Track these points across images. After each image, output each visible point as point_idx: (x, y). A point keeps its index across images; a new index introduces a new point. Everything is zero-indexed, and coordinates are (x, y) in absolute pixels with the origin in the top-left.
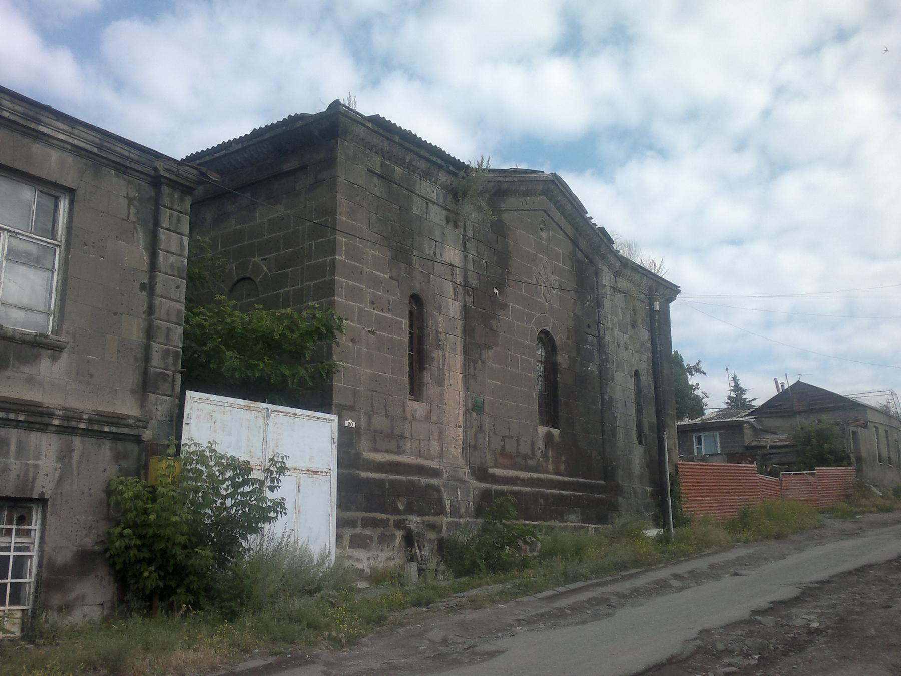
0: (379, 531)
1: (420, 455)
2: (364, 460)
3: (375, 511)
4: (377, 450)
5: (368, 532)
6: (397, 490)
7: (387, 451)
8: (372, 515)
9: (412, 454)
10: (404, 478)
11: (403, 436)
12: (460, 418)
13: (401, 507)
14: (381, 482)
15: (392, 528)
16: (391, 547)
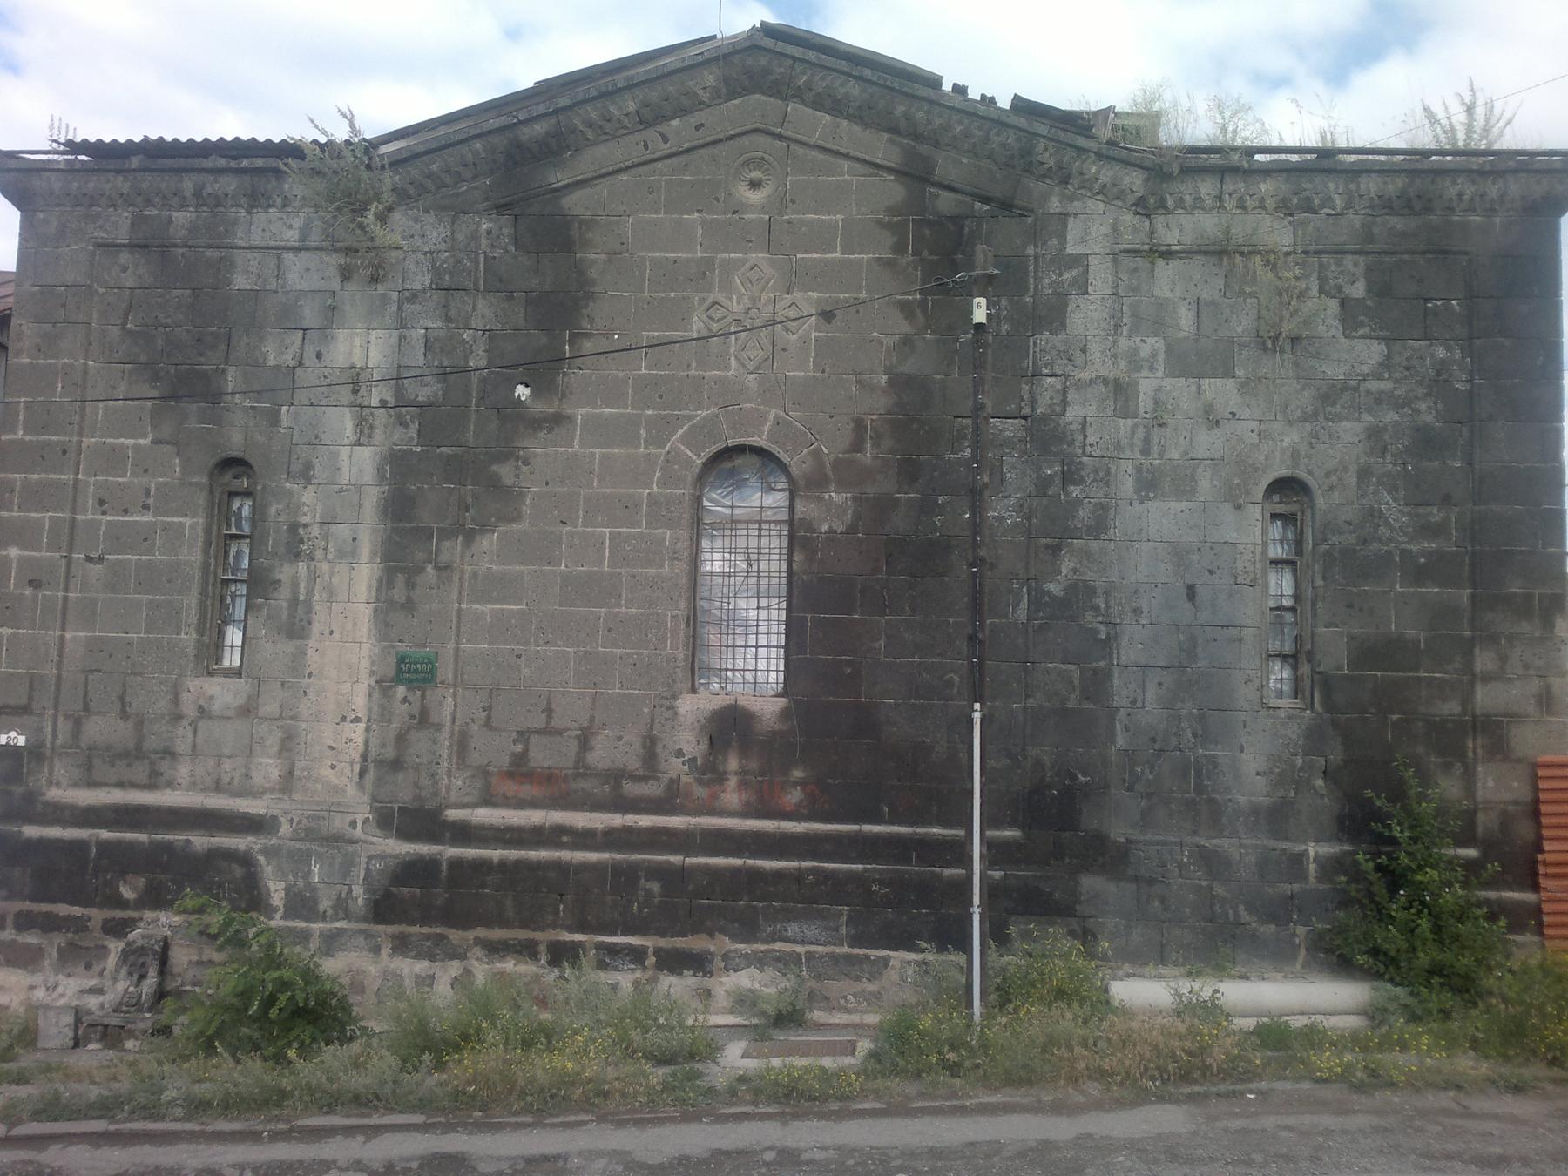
0: (59, 939)
1: (218, 787)
2: (46, 804)
3: (54, 901)
4: (92, 784)
5: (31, 939)
6: (120, 859)
7: (120, 785)
8: (45, 907)
9: (193, 786)
10: (143, 837)
11: (169, 753)
12: (360, 701)
13: (127, 893)
14: (79, 847)
15: (98, 934)
16: (96, 969)
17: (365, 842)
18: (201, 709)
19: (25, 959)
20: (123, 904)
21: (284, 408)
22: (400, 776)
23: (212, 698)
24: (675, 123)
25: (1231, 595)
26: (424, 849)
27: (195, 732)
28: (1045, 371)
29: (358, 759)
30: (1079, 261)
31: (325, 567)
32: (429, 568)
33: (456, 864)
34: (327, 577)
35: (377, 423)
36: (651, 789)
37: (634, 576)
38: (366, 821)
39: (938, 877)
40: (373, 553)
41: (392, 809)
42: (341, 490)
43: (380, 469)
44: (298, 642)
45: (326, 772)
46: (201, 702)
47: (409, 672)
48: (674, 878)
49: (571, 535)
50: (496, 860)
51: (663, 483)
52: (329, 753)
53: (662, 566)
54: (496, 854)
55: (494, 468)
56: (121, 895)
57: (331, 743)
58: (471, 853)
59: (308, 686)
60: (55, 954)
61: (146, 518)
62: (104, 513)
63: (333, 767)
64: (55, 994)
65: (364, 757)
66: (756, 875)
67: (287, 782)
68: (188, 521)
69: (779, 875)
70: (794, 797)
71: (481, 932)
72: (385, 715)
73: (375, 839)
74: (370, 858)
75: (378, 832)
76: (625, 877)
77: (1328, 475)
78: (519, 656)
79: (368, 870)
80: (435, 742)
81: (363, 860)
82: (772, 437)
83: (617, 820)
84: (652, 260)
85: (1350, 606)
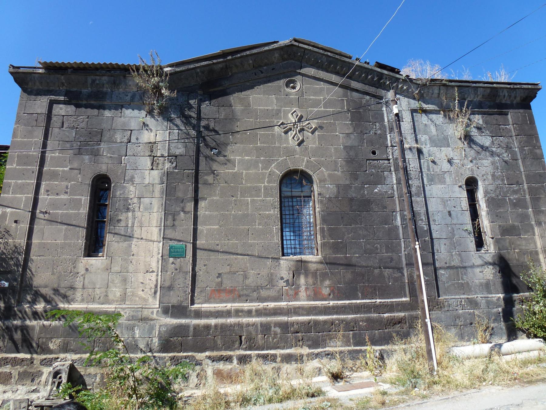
8: (13, 355)
9: (83, 301)
11: (72, 288)
16: (37, 381)
17: (157, 320)
18: (87, 270)
19: (4, 379)
20: (51, 352)
21: (123, 157)
22: (172, 293)
23: (92, 265)
24: (265, 68)
25: (462, 214)
26: (183, 321)
27: (84, 278)
29: (153, 286)
31: (139, 213)
33: (196, 327)
34: (140, 218)
36: (272, 293)
37: (260, 214)
38: (158, 311)
40: (159, 208)
41: (169, 306)
42: (146, 186)
44: (128, 242)
45: (141, 293)
47: (174, 252)
48: (285, 326)
49: (235, 201)
50: (213, 324)
51: (268, 182)
52: (141, 285)
53: (271, 211)
54: (213, 322)
55: (206, 177)
56: (49, 348)
57: (142, 281)
58: (203, 322)
59: (132, 259)
60: (17, 377)
62: (48, 195)
63: (143, 291)
64: (17, 394)
65: (156, 286)
66: (316, 323)
67: (123, 299)
68: (83, 198)
69: (325, 322)
70: (326, 291)
71: (207, 353)
72: (164, 269)
73: (162, 319)
74: (160, 326)
75: (163, 316)
76: (266, 328)
77: (483, 176)
78: (218, 245)
79: (159, 331)
81: (157, 327)
82: (306, 166)
83: (262, 305)
84: (260, 109)
85: (497, 216)
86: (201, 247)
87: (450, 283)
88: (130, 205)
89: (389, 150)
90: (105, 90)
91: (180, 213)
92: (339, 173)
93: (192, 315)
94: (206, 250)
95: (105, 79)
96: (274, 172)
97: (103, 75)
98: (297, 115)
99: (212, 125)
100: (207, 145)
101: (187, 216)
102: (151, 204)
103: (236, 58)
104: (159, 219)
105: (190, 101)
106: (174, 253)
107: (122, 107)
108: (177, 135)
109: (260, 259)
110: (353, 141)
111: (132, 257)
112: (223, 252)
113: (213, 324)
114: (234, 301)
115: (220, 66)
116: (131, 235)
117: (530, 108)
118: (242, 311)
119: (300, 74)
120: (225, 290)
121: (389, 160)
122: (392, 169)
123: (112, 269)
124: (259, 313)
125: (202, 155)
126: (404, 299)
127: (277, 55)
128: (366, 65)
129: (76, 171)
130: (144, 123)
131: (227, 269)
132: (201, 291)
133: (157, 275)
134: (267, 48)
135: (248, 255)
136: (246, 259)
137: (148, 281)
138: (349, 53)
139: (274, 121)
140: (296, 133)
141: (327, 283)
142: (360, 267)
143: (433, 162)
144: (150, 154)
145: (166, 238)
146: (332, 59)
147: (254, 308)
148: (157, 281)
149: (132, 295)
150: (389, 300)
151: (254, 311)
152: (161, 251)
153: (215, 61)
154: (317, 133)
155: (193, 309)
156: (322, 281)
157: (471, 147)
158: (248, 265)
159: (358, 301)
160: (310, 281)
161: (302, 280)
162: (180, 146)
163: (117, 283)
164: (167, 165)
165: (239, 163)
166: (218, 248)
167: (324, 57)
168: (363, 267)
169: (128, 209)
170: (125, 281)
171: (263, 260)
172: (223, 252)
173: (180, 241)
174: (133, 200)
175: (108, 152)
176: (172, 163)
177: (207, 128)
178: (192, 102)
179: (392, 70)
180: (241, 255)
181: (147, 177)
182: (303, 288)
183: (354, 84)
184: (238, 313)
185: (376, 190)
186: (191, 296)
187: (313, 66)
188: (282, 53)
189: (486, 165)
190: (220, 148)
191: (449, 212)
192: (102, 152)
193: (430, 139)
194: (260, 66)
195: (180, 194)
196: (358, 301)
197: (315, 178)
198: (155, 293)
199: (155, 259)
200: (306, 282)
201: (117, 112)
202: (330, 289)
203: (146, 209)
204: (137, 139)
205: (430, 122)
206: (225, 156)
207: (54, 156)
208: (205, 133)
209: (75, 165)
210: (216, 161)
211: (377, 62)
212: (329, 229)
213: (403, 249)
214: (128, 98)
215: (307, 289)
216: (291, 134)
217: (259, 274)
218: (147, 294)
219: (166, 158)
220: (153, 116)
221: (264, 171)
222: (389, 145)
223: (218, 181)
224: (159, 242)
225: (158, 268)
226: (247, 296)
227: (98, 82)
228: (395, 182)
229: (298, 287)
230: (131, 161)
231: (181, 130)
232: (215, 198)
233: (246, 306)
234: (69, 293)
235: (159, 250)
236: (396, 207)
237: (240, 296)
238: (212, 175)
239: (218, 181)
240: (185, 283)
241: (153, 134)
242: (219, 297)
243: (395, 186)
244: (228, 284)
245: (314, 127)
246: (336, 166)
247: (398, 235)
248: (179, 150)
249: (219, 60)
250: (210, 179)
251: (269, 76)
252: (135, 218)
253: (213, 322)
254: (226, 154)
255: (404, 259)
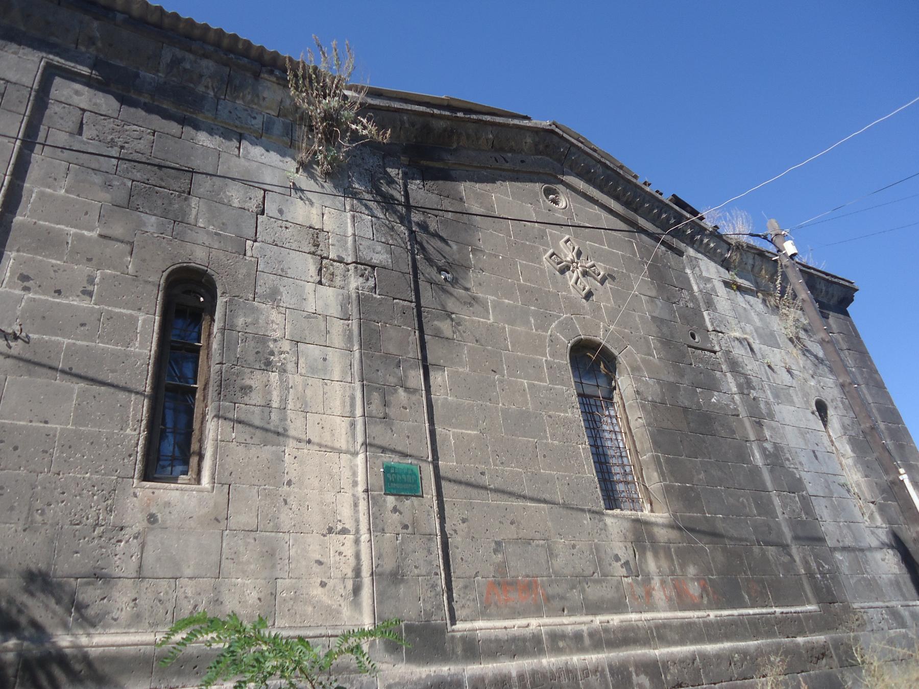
9: (136, 619)
11: (100, 576)
12: (346, 513)
18: (152, 519)
22: (402, 589)
23: (168, 504)
24: (510, 155)
26: (445, 670)
27: (143, 546)
28: (718, 329)
29: (350, 574)
30: (709, 280)
31: (298, 378)
32: (401, 391)
34: (300, 388)
35: (336, 272)
37: (550, 416)
39: (797, 645)
40: (344, 372)
43: (344, 307)
44: (274, 448)
45: (317, 592)
46: (154, 510)
49: (501, 382)
50: (514, 674)
51: (552, 355)
52: (316, 568)
54: (511, 667)
57: (318, 557)
59: (289, 495)
61: (86, 303)
63: (323, 585)
65: (357, 572)
68: (142, 317)
69: (718, 656)
70: (694, 589)
72: (377, 527)
75: (387, 657)
78: (483, 474)
80: (429, 552)
86: (450, 475)
87: (855, 579)
88: (272, 353)
89: (712, 336)
90: (201, 89)
91: (396, 391)
92: (656, 361)
93: (459, 650)
94: (460, 483)
95: (208, 66)
96: (558, 339)
97: (205, 56)
98: (574, 248)
99: (433, 226)
100: (429, 260)
101: (414, 398)
102: (325, 359)
103: (470, 120)
104: (348, 399)
105: (389, 170)
106: (398, 483)
107: (241, 137)
108: (369, 224)
109: (570, 512)
110: (660, 309)
111: (286, 487)
112: (496, 491)
113: (514, 674)
114: (537, 612)
115: (442, 124)
116: (280, 430)
117: (846, 314)
118: (563, 636)
119: (562, 182)
120: (512, 584)
121: (715, 352)
122: (724, 367)
123: (232, 520)
124: (602, 640)
125: (421, 276)
126: (809, 608)
127: (529, 140)
128: (657, 195)
129: (123, 246)
130: (294, 184)
131: (510, 532)
132: (466, 587)
133: (357, 542)
134: (516, 122)
135: (545, 501)
136: (544, 509)
137: (333, 559)
138: (635, 172)
139: (538, 248)
140: (578, 278)
141: (692, 570)
142: (731, 538)
143: (769, 366)
144: (313, 249)
145: (371, 445)
146: (609, 172)
147: (584, 628)
148: (358, 556)
149: (295, 599)
150: (793, 609)
151: (585, 635)
152: (361, 478)
153: (436, 111)
154: (607, 283)
155: (458, 635)
156: (683, 566)
157: (804, 355)
158: (550, 524)
159: (751, 611)
160: (665, 565)
161: (651, 565)
162: (379, 248)
163: (248, 562)
164: (354, 282)
165: (494, 307)
166: (486, 480)
167: (599, 166)
168: (736, 539)
169: (268, 363)
170: (270, 555)
171: (575, 514)
172: (496, 491)
173: (406, 455)
174: (279, 344)
175: (210, 222)
176: (368, 280)
177: (424, 227)
178: (392, 172)
179: (694, 213)
180: (532, 499)
181: (311, 298)
182: (656, 582)
183: (642, 222)
184: (557, 641)
185: (713, 400)
186: (448, 599)
187: (580, 175)
188: (537, 139)
189: (830, 385)
190: (454, 271)
191: (814, 452)
192: (193, 216)
193: (756, 331)
194: (502, 149)
195: (392, 349)
196: (751, 611)
197: (622, 359)
198: (357, 590)
199: (346, 499)
200: (659, 567)
201: (228, 143)
202: (699, 584)
203: (313, 370)
204: (281, 212)
205: (748, 307)
206: (467, 289)
207: (51, 195)
208: (422, 236)
209: (118, 230)
210: (451, 294)
211: (674, 195)
212: (668, 461)
213: (779, 511)
214: (258, 123)
215: (663, 582)
216: (571, 277)
217: (574, 547)
218: (334, 596)
219: (351, 267)
220: (312, 176)
221: (540, 332)
222: (710, 328)
223: (462, 336)
224: (355, 454)
225: (357, 521)
226: (563, 598)
227: (188, 66)
228: (734, 389)
229: (648, 579)
230: (269, 254)
231: (378, 218)
232: (461, 370)
233: (569, 623)
234: (89, 594)
235: (354, 474)
236: (748, 434)
237: (548, 599)
238: (449, 320)
239: (462, 336)
240: (430, 563)
241: (315, 211)
242: (506, 601)
243: (737, 397)
244: (519, 569)
245: (602, 273)
246: (649, 347)
247: (763, 483)
248: (380, 257)
249: (443, 113)
250: (445, 327)
251: (518, 171)
252: (288, 389)
253: (511, 667)
254: (468, 286)
255: (786, 530)
